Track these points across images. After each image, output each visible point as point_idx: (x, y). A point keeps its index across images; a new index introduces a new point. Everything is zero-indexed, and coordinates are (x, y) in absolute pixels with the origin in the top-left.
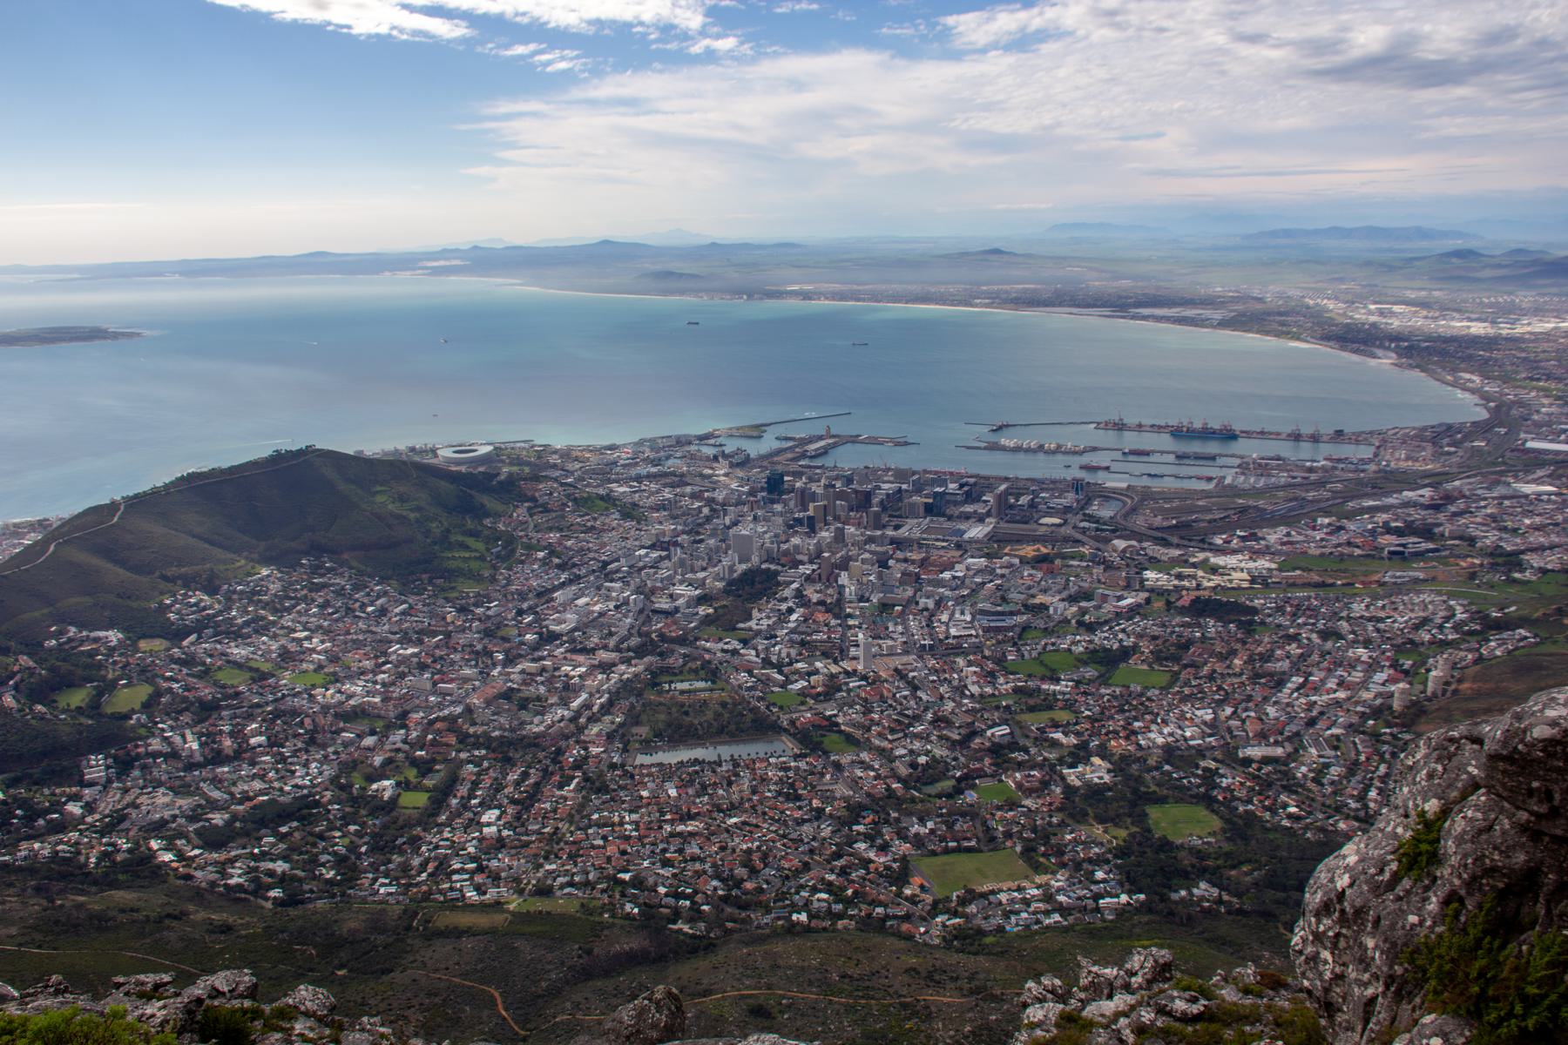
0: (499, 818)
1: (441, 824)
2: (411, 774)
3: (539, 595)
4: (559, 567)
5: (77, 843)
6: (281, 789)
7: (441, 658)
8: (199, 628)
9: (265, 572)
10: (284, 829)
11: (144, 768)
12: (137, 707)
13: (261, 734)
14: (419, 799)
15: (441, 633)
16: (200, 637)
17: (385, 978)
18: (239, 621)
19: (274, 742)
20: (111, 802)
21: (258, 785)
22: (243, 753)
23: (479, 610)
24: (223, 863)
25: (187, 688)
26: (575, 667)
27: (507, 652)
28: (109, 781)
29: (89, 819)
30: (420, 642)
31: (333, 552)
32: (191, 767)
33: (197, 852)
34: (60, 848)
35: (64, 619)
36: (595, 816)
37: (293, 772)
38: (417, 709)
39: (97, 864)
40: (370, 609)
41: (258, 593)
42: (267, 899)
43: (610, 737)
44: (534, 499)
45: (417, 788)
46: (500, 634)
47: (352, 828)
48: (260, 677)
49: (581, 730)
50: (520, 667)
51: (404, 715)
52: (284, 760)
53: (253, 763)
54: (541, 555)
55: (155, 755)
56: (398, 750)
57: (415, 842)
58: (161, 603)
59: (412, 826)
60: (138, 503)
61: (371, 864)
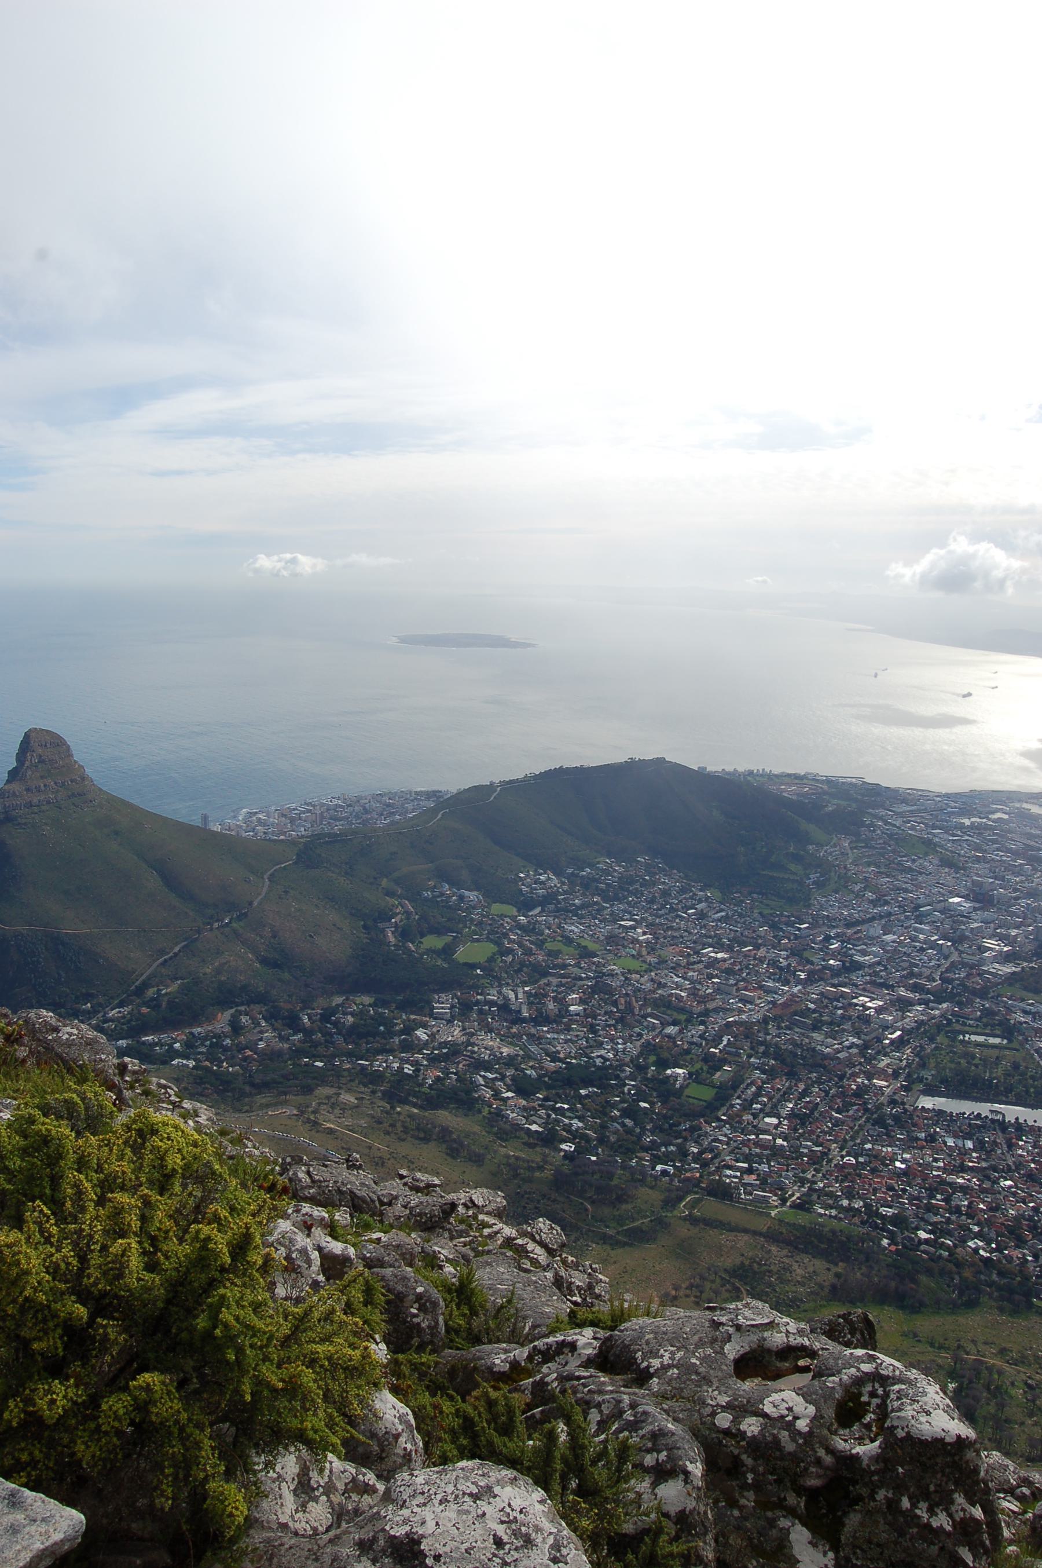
0: (776, 1127)
4: (871, 902)
8: (543, 902)
10: (583, 1092)
11: (481, 1012)
14: (707, 1094)
16: (543, 911)
22: (560, 1019)
26: (872, 999)
27: (811, 974)
30: (729, 949)
33: (510, 1094)
36: (868, 1146)
43: (896, 1075)
48: (586, 954)
49: (869, 1060)
51: (706, 1013)
55: (492, 1003)
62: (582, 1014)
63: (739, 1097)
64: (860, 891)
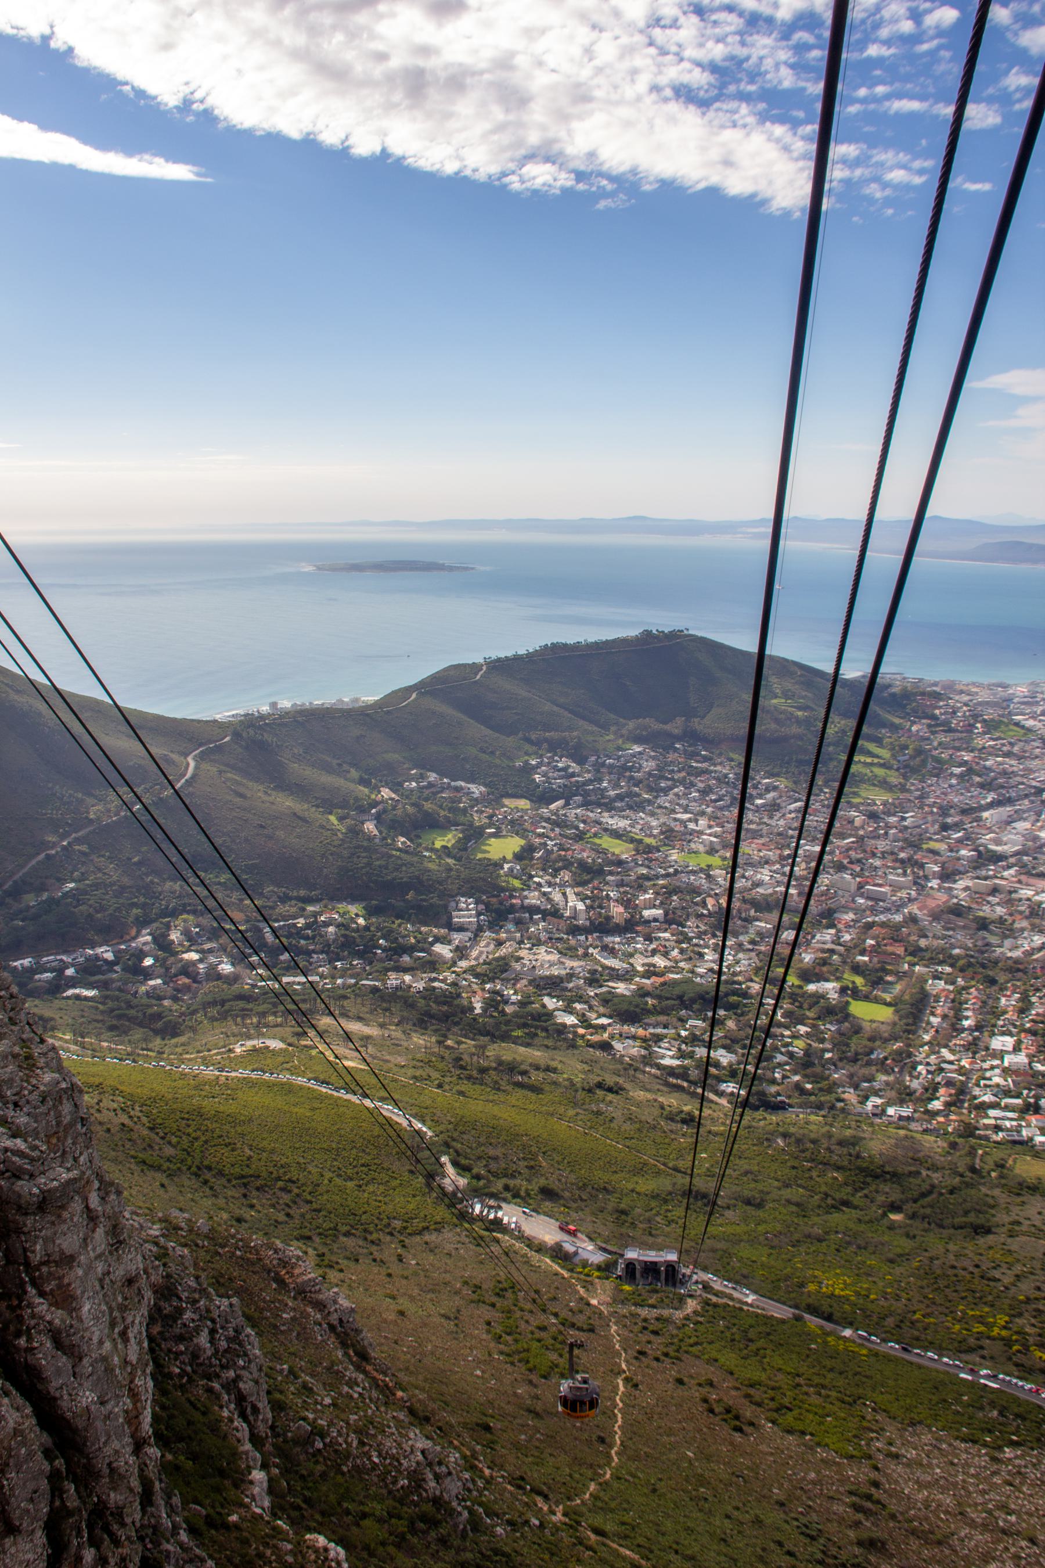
0: (1017, 1049)
1: (929, 1043)
2: (859, 981)
3: (964, 812)
4: (982, 786)
5: (454, 984)
6: (693, 972)
7: (859, 861)
8: (567, 794)
9: (637, 748)
11: (518, 922)
12: (509, 857)
13: (654, 907)
15: (851, 836)
16: (567, 804)
17: (983, 1241)
18: (612, 793)
19: (670, 920)
20: (483, 950)
21: (660, 962)
23: (893, 820)
24: (644, 1040)
25: (562, 848)
26: (1037, 894)
28: (479, 930)
29: (464, 964)
31: (709, 742)
32: (575, 930)
33: (604, 1021)
34: (436, 984)
35: (425, 765)
37: (701, 955)
38: (846, 909)
39: (485, 1010)
40: (759, 802)
41: (630, 769)
42: (721, 1094)
44: (934, 717)
45: (867, 998)
46: (925, 846)
47: (803, 1029)
50: (961, 884)
52: (689, 940)
53: (649, 938)
54: (957, 771)
55: (533, 910)
56: (832, 952)
57: (905, 1061)
58: (526, 762)
59: (886, 1041)
60: (500, 666)
61: (851, 1076)
62: (661, 919)
63: (933, 1014)
64: (961, 776)
